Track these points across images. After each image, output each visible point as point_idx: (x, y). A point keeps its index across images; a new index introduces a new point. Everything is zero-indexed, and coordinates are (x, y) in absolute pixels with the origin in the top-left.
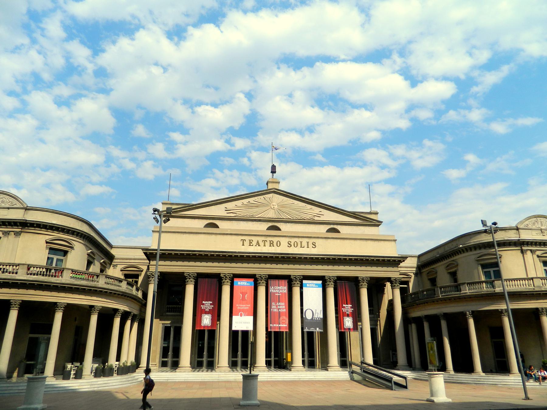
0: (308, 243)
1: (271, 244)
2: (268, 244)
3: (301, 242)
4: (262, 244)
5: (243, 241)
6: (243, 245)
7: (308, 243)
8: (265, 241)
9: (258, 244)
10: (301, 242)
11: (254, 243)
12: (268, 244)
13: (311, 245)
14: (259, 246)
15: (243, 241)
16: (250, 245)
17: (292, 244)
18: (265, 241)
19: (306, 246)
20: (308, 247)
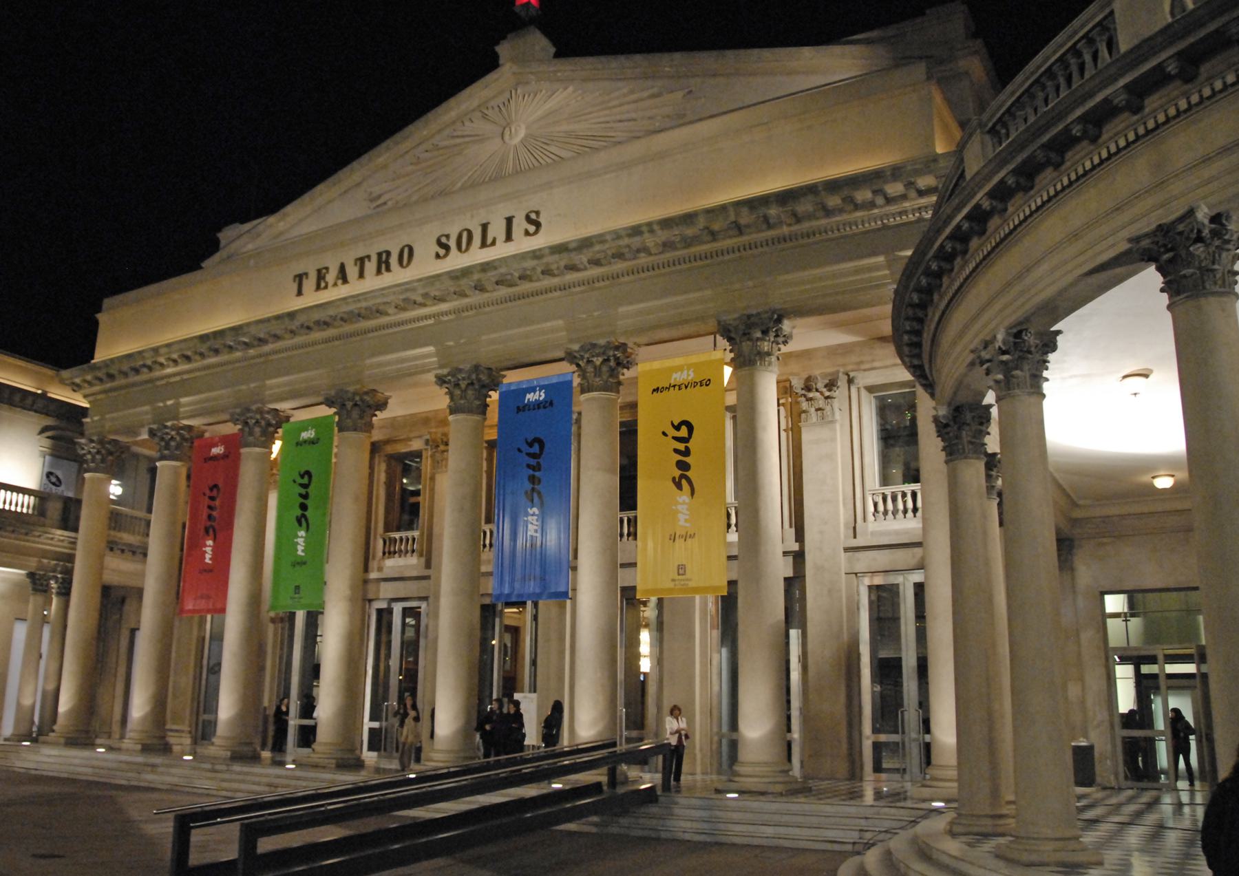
0: (509, 221)
1: (383, 263)
2: (371, 267)
3: (485, 227)
4: (352, 271)
5: (300, 278)
6: (300, 293)
7: (509, 221)
8: (361, 261)
9: (343, 276)
10: (485, 227)
11: (331, 277)
12: (371, 267)
13: (520, 225)
14: (345, 281)
15: (300, 278)
16: (318, 288)
17: (452, 243)
18: (361, 261)
19: (501, 236)
20: (509, 238)
